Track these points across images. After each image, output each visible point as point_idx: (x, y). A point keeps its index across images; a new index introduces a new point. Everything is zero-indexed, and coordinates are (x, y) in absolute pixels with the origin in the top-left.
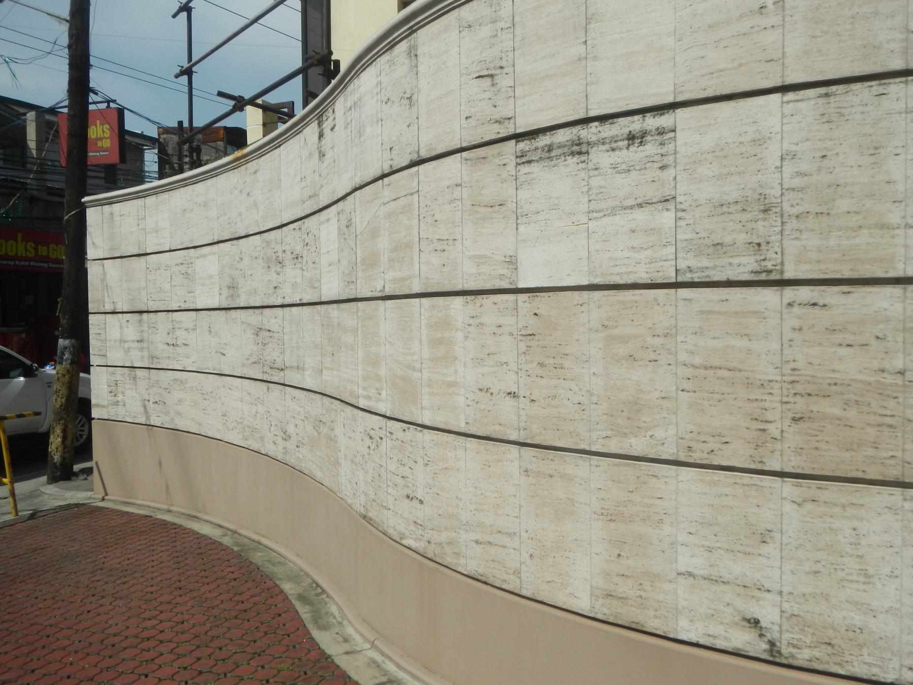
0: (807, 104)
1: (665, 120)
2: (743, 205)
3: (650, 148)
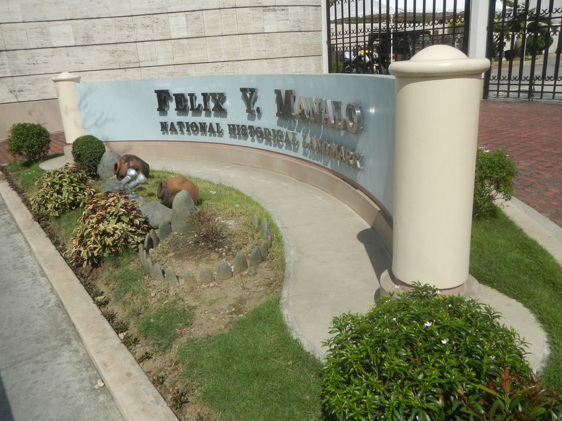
0: (302, 8)
2: (297, 21)
3: (285, 12)
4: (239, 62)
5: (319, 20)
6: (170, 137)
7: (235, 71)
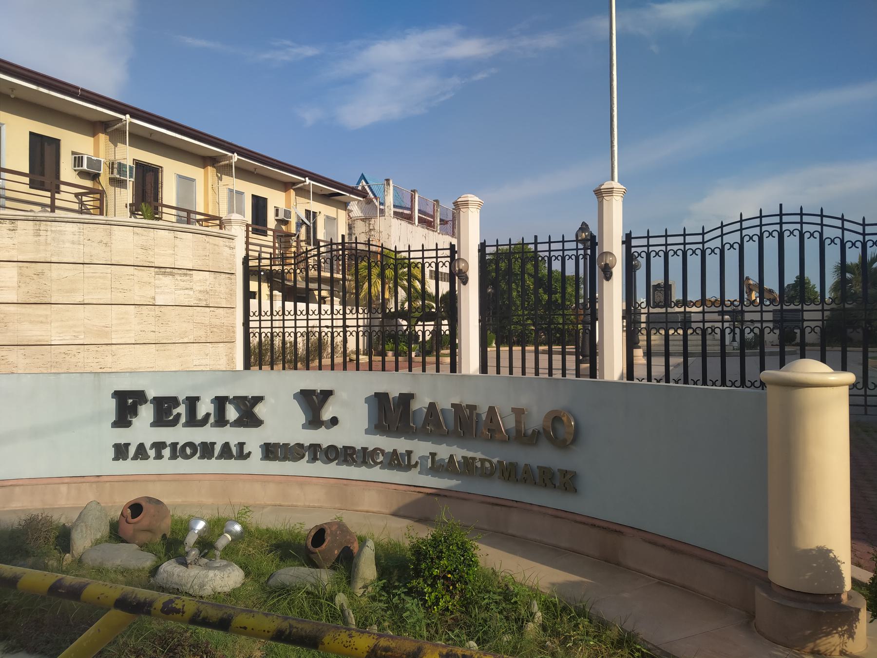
1: (191, 272)
3: (188, 278)
4: (109, 347)
5: (232, 293)
6: (129, 467)
7: (100, 360)
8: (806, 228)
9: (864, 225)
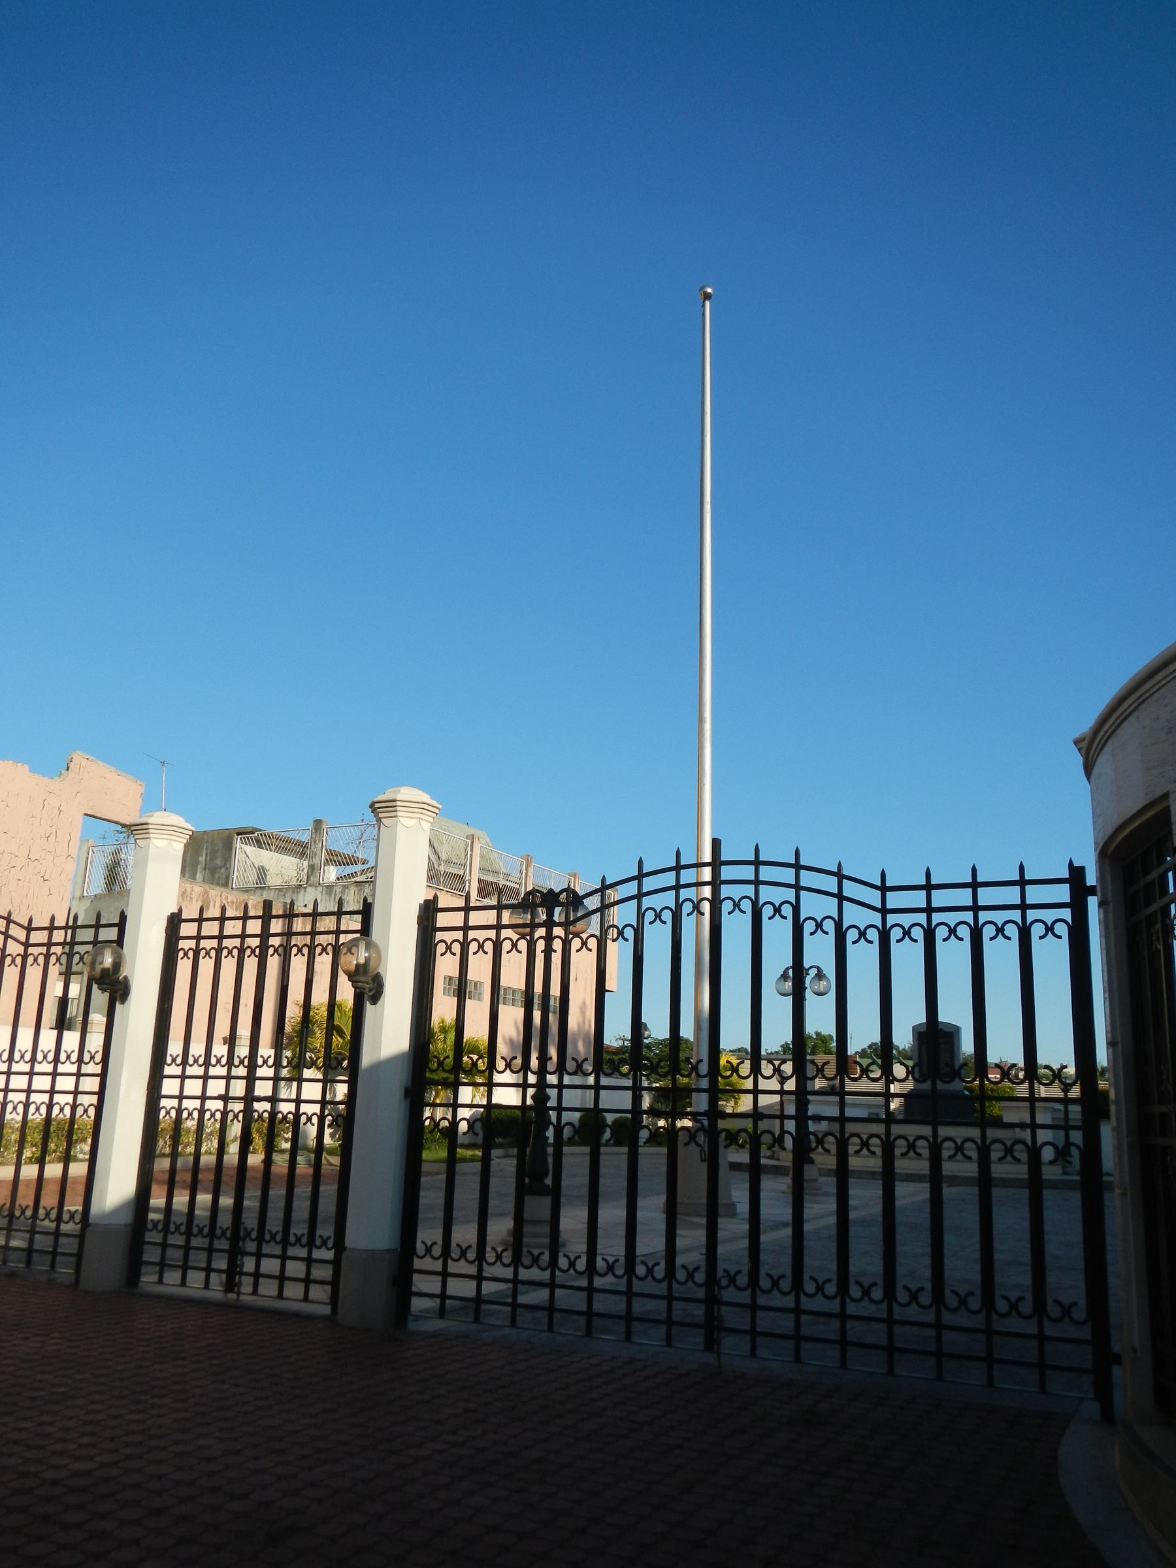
8: (766, 893)
9: (884, 889)
